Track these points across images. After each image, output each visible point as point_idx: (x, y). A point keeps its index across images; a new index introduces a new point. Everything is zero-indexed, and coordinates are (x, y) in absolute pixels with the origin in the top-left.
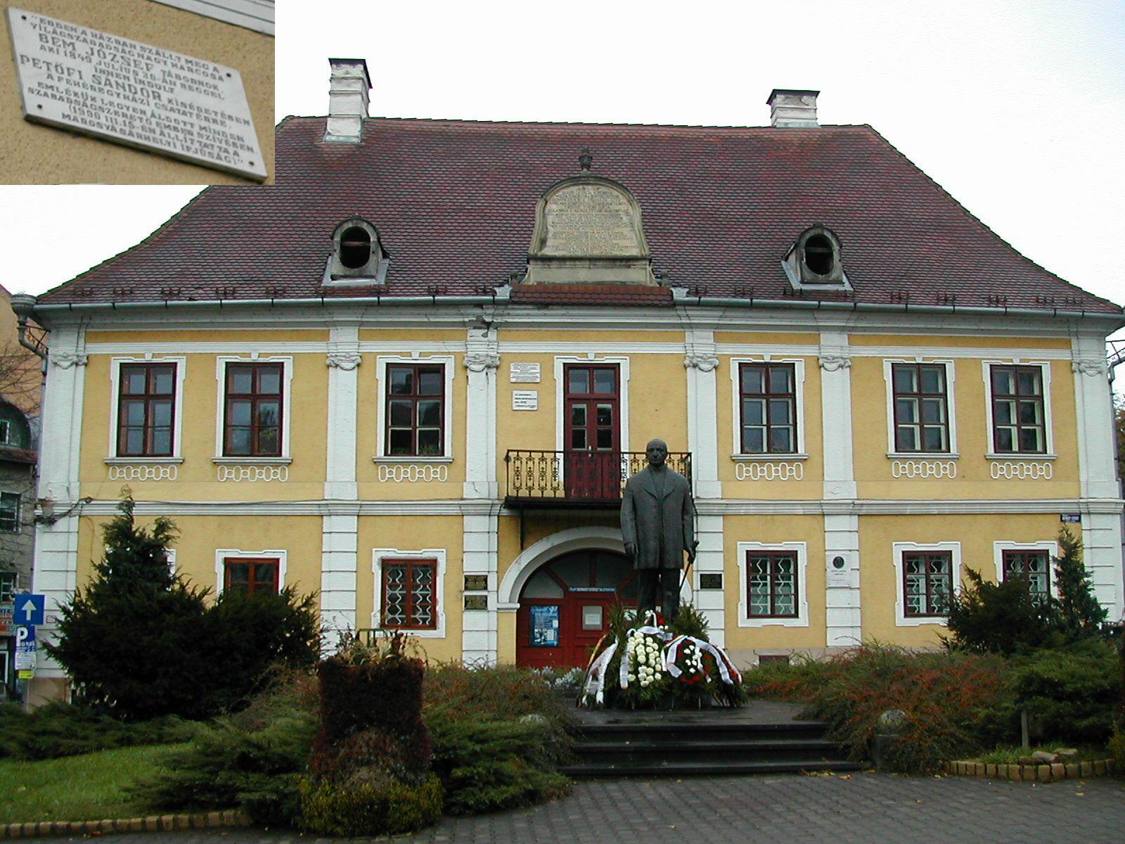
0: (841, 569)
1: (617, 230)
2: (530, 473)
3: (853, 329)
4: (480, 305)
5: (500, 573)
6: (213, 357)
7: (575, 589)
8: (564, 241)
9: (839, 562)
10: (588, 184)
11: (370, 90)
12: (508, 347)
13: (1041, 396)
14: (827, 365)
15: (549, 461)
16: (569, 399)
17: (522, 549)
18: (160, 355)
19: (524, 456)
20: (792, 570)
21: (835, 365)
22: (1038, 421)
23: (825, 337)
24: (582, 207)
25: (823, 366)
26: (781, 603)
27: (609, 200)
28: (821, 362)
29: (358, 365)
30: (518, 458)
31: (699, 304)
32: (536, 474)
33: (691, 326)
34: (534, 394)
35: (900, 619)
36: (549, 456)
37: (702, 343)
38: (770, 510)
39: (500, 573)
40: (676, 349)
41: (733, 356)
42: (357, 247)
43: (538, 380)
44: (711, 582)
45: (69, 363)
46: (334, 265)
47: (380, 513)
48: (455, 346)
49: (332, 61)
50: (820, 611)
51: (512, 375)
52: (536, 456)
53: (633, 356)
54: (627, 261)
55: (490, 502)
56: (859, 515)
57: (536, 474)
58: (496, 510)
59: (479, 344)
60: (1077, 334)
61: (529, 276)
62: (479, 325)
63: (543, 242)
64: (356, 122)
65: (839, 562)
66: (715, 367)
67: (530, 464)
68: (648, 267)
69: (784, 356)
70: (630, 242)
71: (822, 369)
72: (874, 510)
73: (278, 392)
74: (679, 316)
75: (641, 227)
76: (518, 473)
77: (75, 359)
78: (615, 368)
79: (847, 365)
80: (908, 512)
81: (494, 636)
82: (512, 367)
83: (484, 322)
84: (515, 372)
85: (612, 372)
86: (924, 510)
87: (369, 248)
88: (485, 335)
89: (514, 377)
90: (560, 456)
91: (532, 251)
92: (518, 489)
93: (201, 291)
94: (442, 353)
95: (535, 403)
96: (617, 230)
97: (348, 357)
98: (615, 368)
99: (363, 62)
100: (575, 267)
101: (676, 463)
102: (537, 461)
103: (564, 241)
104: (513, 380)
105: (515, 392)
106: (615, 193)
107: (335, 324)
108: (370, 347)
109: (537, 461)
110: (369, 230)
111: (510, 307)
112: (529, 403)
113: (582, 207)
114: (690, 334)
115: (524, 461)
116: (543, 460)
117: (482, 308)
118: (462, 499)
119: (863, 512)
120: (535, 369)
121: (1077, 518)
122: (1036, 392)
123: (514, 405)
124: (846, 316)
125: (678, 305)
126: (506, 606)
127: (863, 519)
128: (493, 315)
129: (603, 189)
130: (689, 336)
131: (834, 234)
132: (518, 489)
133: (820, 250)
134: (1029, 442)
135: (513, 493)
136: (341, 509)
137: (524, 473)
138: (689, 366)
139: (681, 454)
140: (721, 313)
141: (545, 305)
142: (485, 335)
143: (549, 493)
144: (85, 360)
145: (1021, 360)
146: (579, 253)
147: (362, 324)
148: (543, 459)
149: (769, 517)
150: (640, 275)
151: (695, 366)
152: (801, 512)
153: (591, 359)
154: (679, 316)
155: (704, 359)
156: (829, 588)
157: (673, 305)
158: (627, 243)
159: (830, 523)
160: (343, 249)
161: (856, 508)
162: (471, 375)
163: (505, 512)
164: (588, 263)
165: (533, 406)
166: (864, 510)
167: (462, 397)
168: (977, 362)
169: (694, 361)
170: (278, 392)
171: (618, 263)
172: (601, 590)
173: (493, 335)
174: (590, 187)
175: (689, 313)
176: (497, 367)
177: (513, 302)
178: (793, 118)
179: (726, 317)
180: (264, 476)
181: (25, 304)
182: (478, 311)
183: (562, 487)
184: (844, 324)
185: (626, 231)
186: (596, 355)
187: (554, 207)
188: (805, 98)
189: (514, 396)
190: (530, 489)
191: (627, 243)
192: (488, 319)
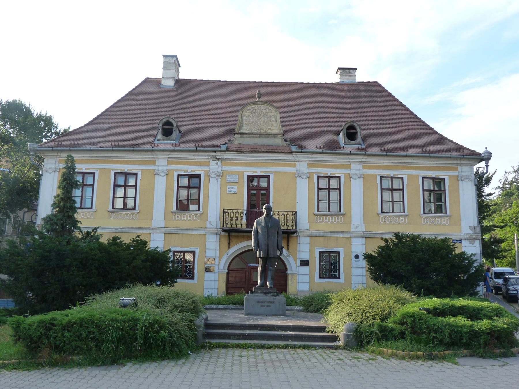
2: (232, 218)
3: (364, 162)
4: (215, 151)
5: (220, 257)
6: (109, 170)
7: (250, 265)
8: (249, 127)
9: (357, 257)
10: (260, 105)
11: (180, 68)
12: (226, 168)
13: (445, 190)
14: (353, 177)
16: (249, 189)
18: (89, 169)
20: (338, 260)
21: (357, 177)
22: (443, 200)
23: (353, 166)
24: (257, 114)
25: (352, 177)
26: (324, 272)
27: (267, 111)
28: (351, 176)
29: (167, 174)
31: (301, 152)
32: (234, 218)
34: (236, 187)
36: (240, 212)
37: (303, 167)
38: (329, 235)
39: (220, 257)
40: (292, 170)
41: (316, 173)
42: (168, 129)
43: (237, 182)
44: (304, 263)
45: (52, 171)
46: (160, 136)
47: (174, 232)
48: (205, 168)
49: (164, 56)
50: (349, 276)
52: (235, 211)
54: (275, 135)
55: (217, 229)
58: (219, 232)
59: (214, 167)
60: (461, 165)
61: (235, 141)
62: (214, 159)
63: (241, 127)
64: (173, 80)
66: (308, 178)
67: (232, 214)
69: (336, 173)
70: (276, 128)
72: (372, 236)
73: (134, 184)
76: (227, 218)
77: (54, 170)
78: (268, 177)
81: (217, 283)
82: (227, 176)
83: (217, 159)
84: (228, 178)
87: (173, 129)
88: (217, 164)
89: (228, 180)
91: (236, 131)
93: (105, 144)
94: (200, 170)
95: (236, 190)
97: (163, 171)
98: (268, 177)
99: (176, 57)
100: (253, 137)
101: (290, 215)
102: (235, 213)
103: (249, 127)
104: (228, 181)
105: (228, 186)
106: (270, 108)
107: (158, 158)
108: (171, 167)
109: (235, 213)
110: (173, 122)
111: (227, 152)
113: (257, 114)
114: (298, 164)
116: (237, 213)
117: (216, 153)
118: (206, 228)
120: (236, 177)
121: (460, 241)
122: (443, 189)
124: (362, 157)
126: (222, 271)
128: (220, 156)
129: (266, 106)
130: (298, 165)
131: (358, 125)
133: (352, 131)
134: (440, 209)
136: (158, 231)
139: (293, 212)
140: (311, 156)
141: (242, 152)
142: (217, 164)
143: (239, 226)
144: (59, 171)
145: (436, 176)
146: (255, 132)
147: (169, 158)
148: (237, 213)
149: (328, 238)
150: (279, 141)
151: (300, 177)
152: (342, 236)
155: (304, 174)
156: (353, 267)
157: (291, 153)
158: (274, 128)
159: (354, 241)
160: (163, 129)
162: (211, 179)
163: (223, 233)
164: (258, 136)
165: (235, 192)
166: (368, 236)
167: (207, 187)
168: (417, 176)
170: (134, 184)
171: (270, 136)
173: (220, 164)
174: (260, 106)
175: (298, 155)
176: (221, 176)
177: (227, 150)
178: (347, 80)
180: (128, 217)
181: (33, 147)
182: (214, 154)
184: (361, 161)
185: (274, 123)
187: (246, 113)
188: (351, 71)
189: (228, 188)
191: (274, 128)
192: (218, 157)
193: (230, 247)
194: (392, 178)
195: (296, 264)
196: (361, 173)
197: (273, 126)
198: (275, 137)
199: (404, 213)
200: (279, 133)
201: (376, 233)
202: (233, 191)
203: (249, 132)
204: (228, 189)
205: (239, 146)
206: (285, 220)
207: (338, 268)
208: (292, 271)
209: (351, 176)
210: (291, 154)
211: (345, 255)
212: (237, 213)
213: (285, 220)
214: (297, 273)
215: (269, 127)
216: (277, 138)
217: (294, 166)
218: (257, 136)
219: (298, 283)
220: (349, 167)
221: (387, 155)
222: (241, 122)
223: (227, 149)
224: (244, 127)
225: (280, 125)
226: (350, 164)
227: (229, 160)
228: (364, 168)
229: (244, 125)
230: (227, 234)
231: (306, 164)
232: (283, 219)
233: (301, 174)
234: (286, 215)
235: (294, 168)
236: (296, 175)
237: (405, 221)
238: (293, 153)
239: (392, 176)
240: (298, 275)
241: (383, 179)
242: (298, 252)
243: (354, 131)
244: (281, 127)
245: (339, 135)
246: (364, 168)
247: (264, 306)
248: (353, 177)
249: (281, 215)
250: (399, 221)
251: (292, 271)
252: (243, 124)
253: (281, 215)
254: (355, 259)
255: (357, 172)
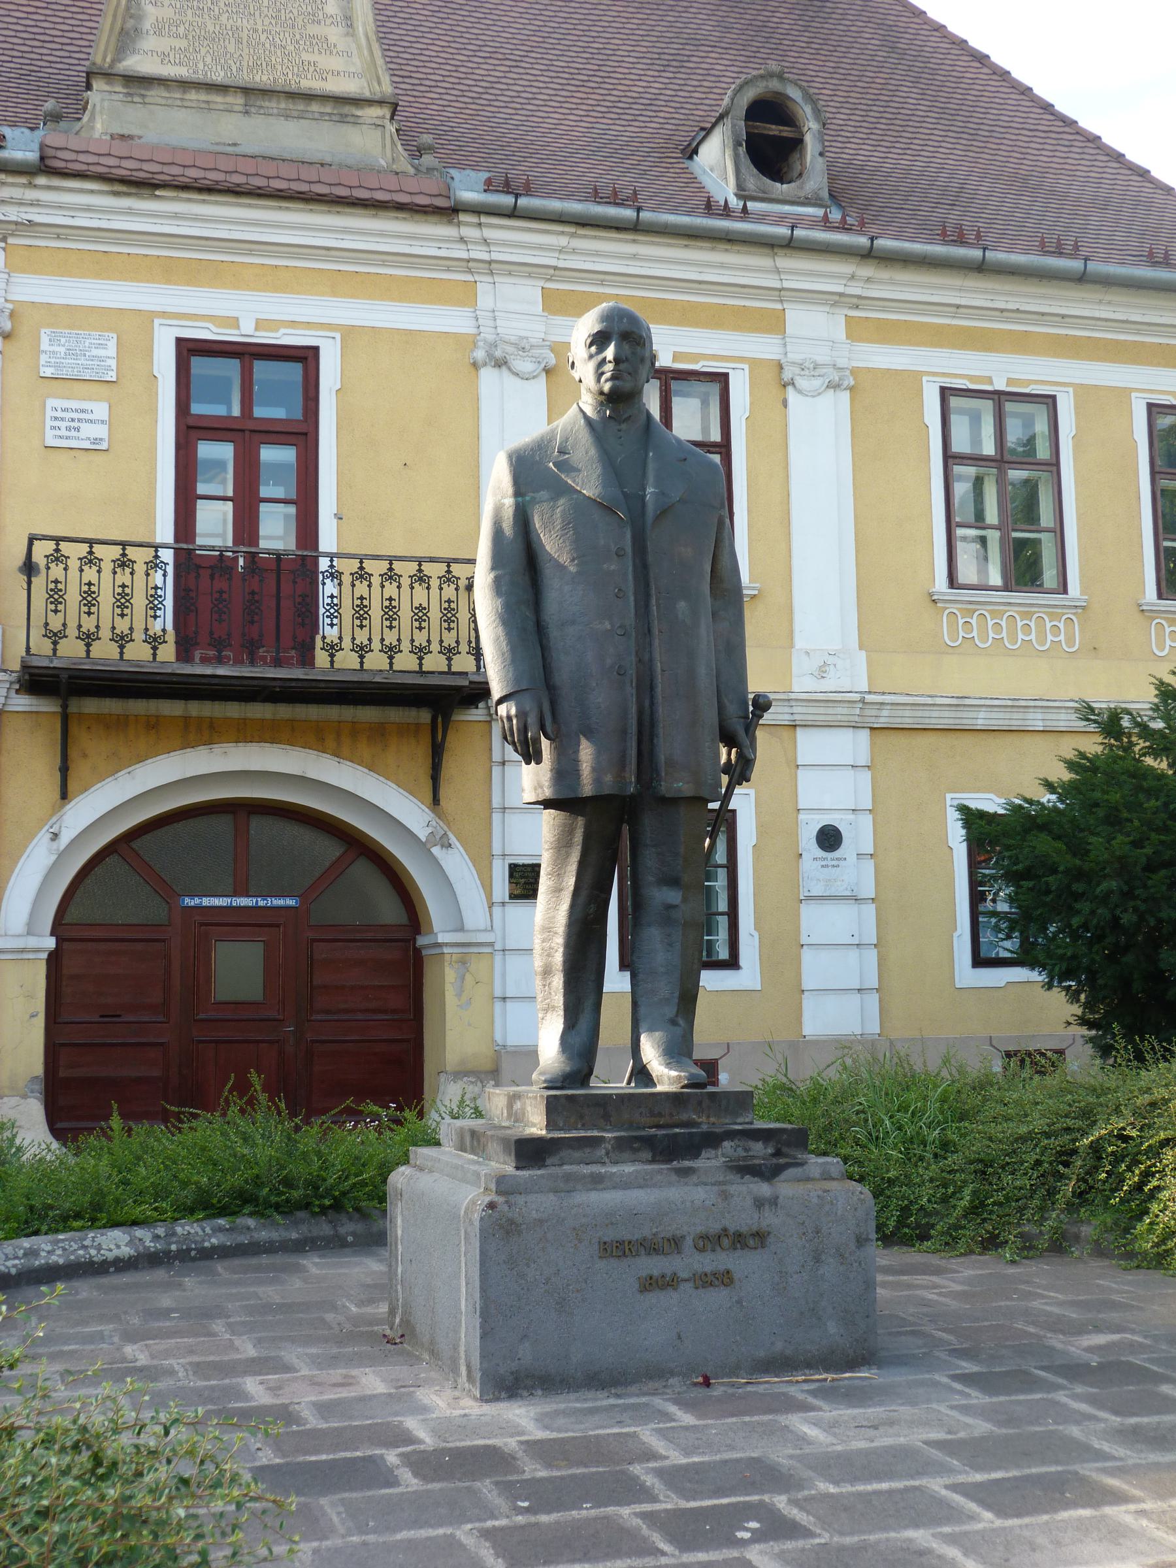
0: (836, 854)
1: (313, 29)
2: (89, 598)
3: (858, 302)
7: (197, 901)
8: (183, 44)
9: (829, 838)
14: (799, 382)
15: (140, 568)
16: (189, 427)
17: (64, 795)
19: (72, 552)
23: (799, 318)
25: (792, 383)
28: (787, 375)
30: (57, 557)
31: (513, 213)
32: (106, 599)
33: (490, 267)
34: (100, 410)
35: (967, 975)
36: (139, 556)
43: (112, 376)
51: (43, 358)
52: (108, 554)
53: (349, 334)
56: (871, 728)
57: (106, 599)
63: (127, 39)
65: (829, 838)
66: (548, 371)
67: (90, 574)
68: (387, 122)
71: (790, 389)
72: (907, 718)
74: (462, 240)
75: (371, 28)
76: (56, 597)
78: (307, 357)
79: (846, 383)
80: (980, 723)
82: (45, 345)
85: (294, 371)
86: (1014, 720)
90: (167, 556)
91: (101, 56)
92: (55, 637)
95: (102, 431)
96: (313, 29)
98: (307, 357)
100: (208, 107)
102: (107, 567)
103: (183, 44)
104: (48, 372)
105: (51, 403)
109: (107, 567)
111: (41, 180)
112: (91, 431)
115: (74, 564)
116: (123, 565)
119: (882, 722)
120: (103, 346)
123: (49, 434)
125: (465, 211)
126: (19, 943)
127: (882, 738)
132: (55, 637)
133: (774, 130)
135: (42, 646)
137: (73, 596)
138: (485, 364)
140: (563, 241)
143: (138, 652)
146: (219, 77)
151: (501, 364)
153: (247, 332)
154: (462, 240)
155: (522, 348)
157: (450, 212)
161: (867, 712)
169: (498, 353)
171: (315, 107)
172: (261, 903)
175: (488, 233)
179: (574, 251)
183: (171, 637)
184: (840, 289)
185: (335, 34)
186: (260, 324)
189: (49, 413)
190: (89, 638)
193: (71, 786)
194: (999, 398)
195: (487, 886)
196: (842, 362)
197: (330, 49)
198: (343, 120)
199: (1065, 592)
200: (367, 95)
201: (929, 701)
202: (82, 434)
203: (181, 72)
204: (49, 423)
205: (119, 148)
206: (435, 614)
207: (723, 906)
208: (461, 929)
209: (787, 375)
210: (450, 222)
211: (763, 829)
212: (123, 563)
213: (435, 614)
214: (491, 944)
215: (305, 56)
216: (356, 122)
217: (466, 297)
218: (230, 99)
219: (498, 1005)
220: (775, 324)
221: (981, 268)
222: (128, 8)
223: (42, 158)
224: (149, 43)
225: (376, 47)
226: (779, 306)
227: (58, 237)
228: (856, 331)
229: (147, 25)
230: (47, 706)
231: (530, 293)
232: (420, 608)
233: (510, 349)
234: (435, 583)
235: (467, 312)
236: (480, 354)
237: (1070, 641)
238: (463, 217)
239: (1000, 385)
240: (498, 958)
241: (954, 402)
242: (496, 817)
243: (786, 132)
244: (380, 62)
245: (690, 158)
246: (856, 331)
247: (668, 1283)
248: (801, 382)
249: (405, 582)
250: (1042, 639)
251: (461, 929)
252: (139, 18)
253: (405, 582)
254: (820, 853)
255: (822, 355)
